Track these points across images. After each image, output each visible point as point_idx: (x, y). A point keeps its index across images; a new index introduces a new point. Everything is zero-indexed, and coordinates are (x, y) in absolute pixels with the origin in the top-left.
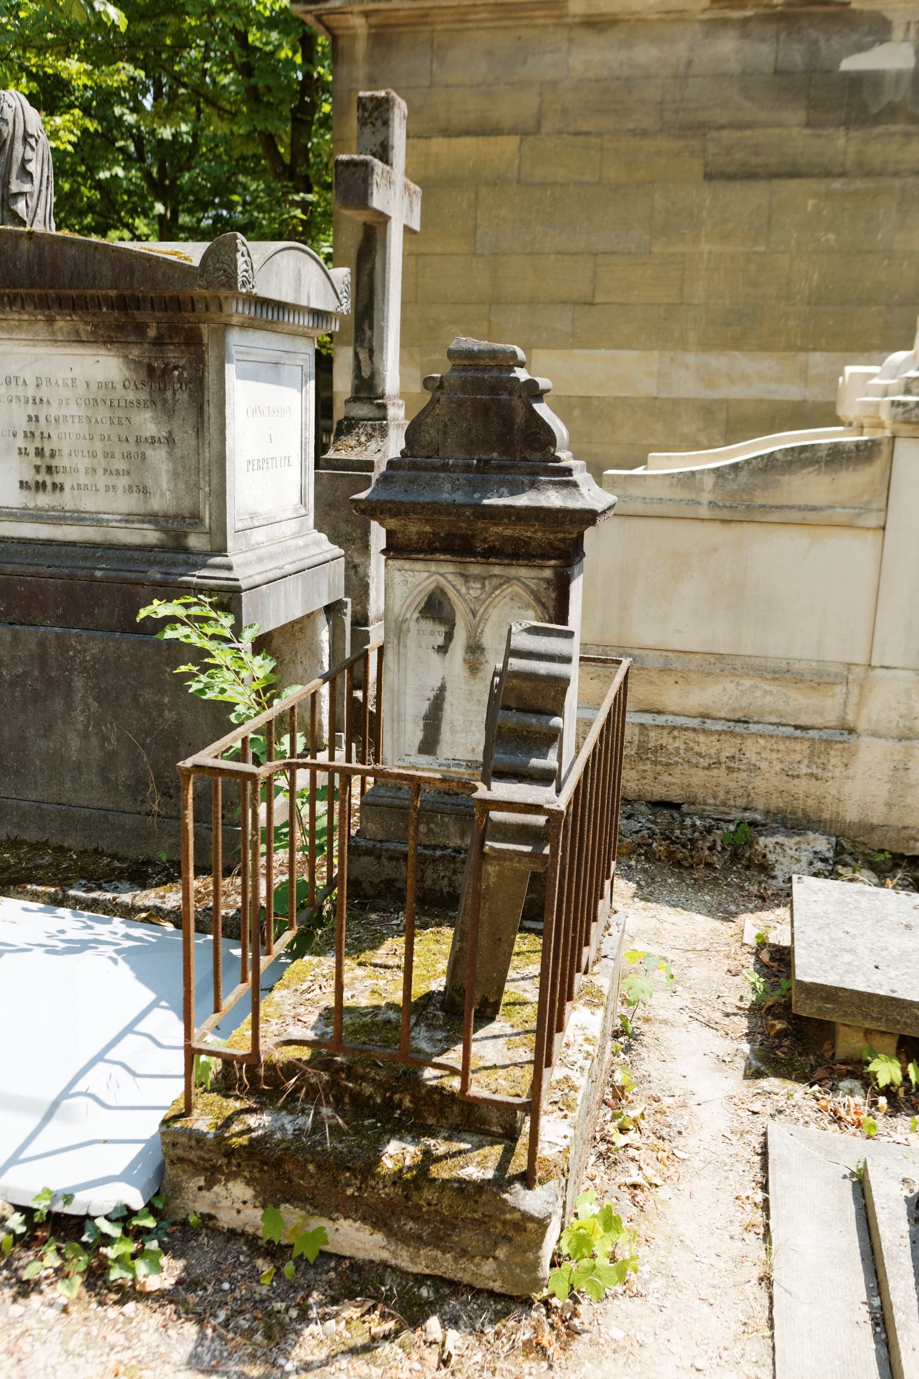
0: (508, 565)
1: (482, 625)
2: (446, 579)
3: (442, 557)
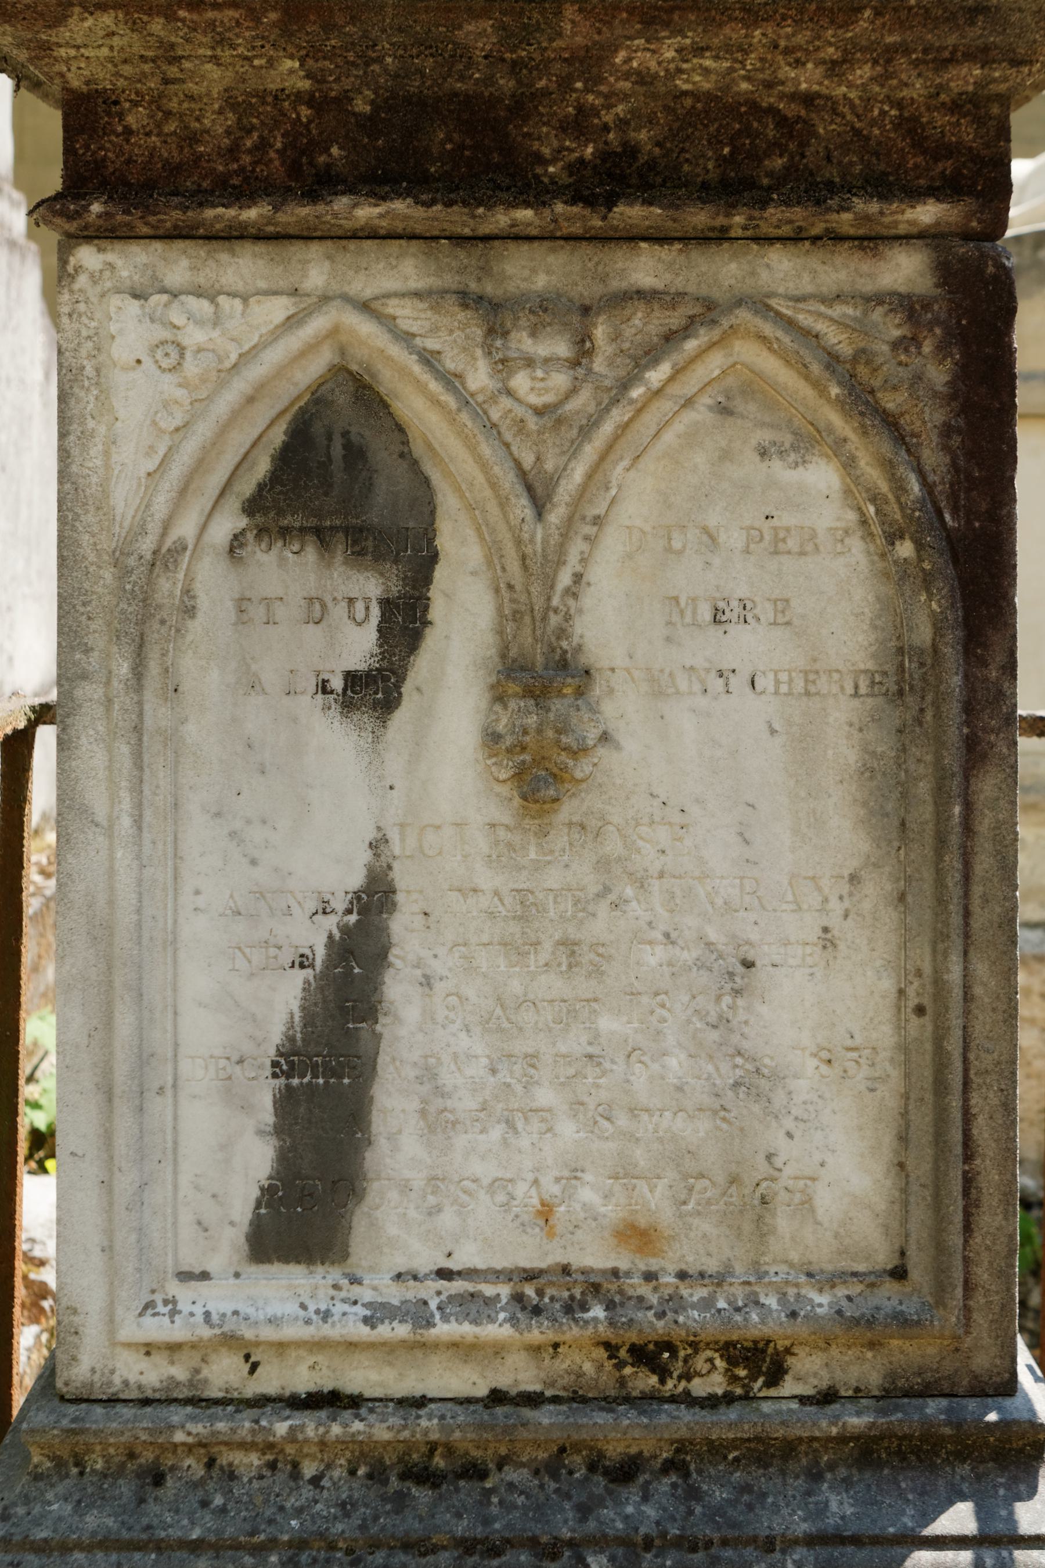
0: (719, 237)
1: (576, 548)
2: (387, 322)
3: (367, 213)
